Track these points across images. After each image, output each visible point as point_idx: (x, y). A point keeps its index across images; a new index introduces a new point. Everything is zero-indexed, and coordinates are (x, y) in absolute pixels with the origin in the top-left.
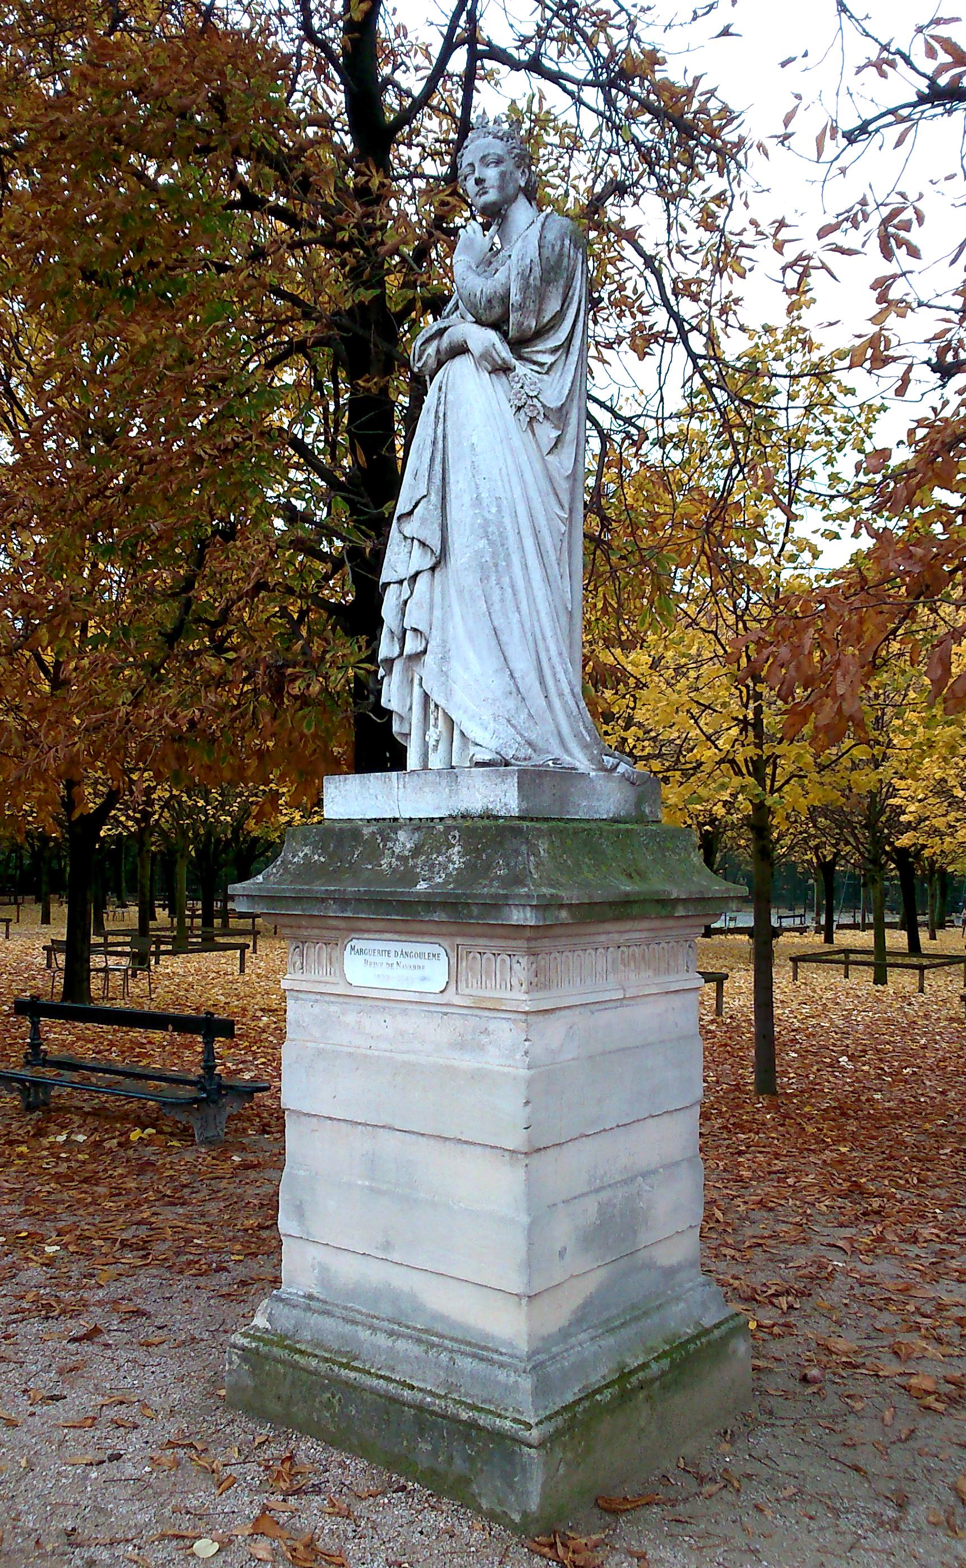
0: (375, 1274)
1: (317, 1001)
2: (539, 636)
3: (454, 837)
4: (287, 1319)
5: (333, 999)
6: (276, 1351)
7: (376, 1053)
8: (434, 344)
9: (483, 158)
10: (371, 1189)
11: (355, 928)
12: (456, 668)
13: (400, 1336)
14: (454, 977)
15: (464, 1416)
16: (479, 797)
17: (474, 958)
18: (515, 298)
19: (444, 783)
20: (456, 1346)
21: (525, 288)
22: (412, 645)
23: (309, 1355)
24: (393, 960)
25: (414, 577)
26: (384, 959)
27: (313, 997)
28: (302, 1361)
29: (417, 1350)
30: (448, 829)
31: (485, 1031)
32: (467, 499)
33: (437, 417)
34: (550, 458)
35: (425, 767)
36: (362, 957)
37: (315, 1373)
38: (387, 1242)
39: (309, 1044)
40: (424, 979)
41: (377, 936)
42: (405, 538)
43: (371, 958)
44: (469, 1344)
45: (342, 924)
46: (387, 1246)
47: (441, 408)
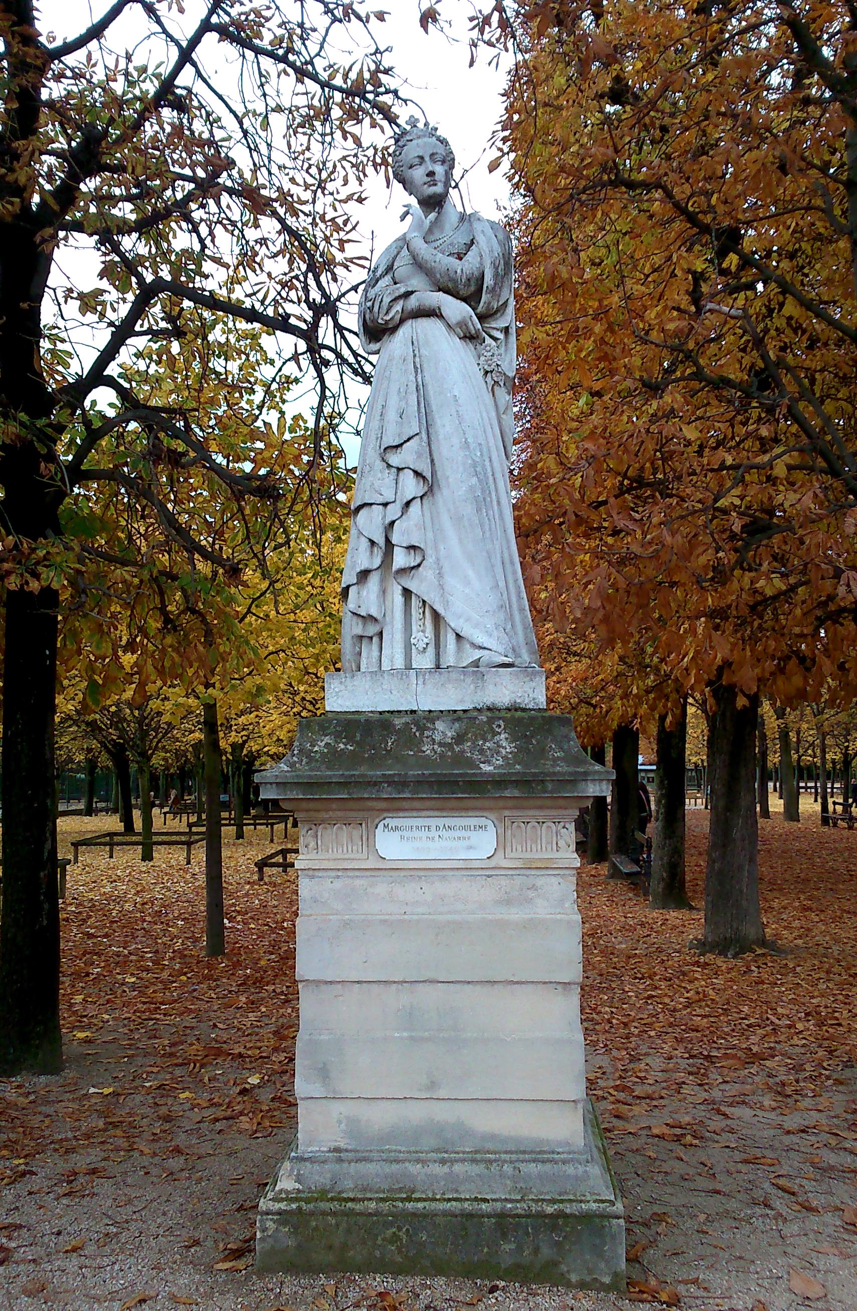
0: (416, 1114)
1: (338, 877)
2: (507, 561)
3: (499, 726)
5: (357, 873)
6: (324, 1206)
7: (415, 917)
8: (401, 302)
9: (432, 155)
10: (411, 1038)
11: (395, 807)
12: (451, 582)
13: (453, 1162)
14: (502, 844)
15: (550, 1209)
16: (507, 692)
17: (519, 827)
18: (488, 281)
20: (514, 1157)
21: (496, 275)
22: (400, 559)
23: (363, 1200)
24: (434, 833)
25: (408, 504)
26: (424, 834)
27: (333, 874)
28: (358, 1207)
29: (476, 1170)
30: (491, 721)
31: (534, 887)
32: (455, 441)
33: (415, 367)
34: (504, 416)
35: (409, 667)
36: (398, 834)
37: (377, 1213)
38: (432, 1082)
40: (470, 848)
41: (415, 814)
42: (389, 466)
43: (406, 834)
44: (524, 1152)
45: (383, 805)
46: (433, 1085)
47: (417, 359)
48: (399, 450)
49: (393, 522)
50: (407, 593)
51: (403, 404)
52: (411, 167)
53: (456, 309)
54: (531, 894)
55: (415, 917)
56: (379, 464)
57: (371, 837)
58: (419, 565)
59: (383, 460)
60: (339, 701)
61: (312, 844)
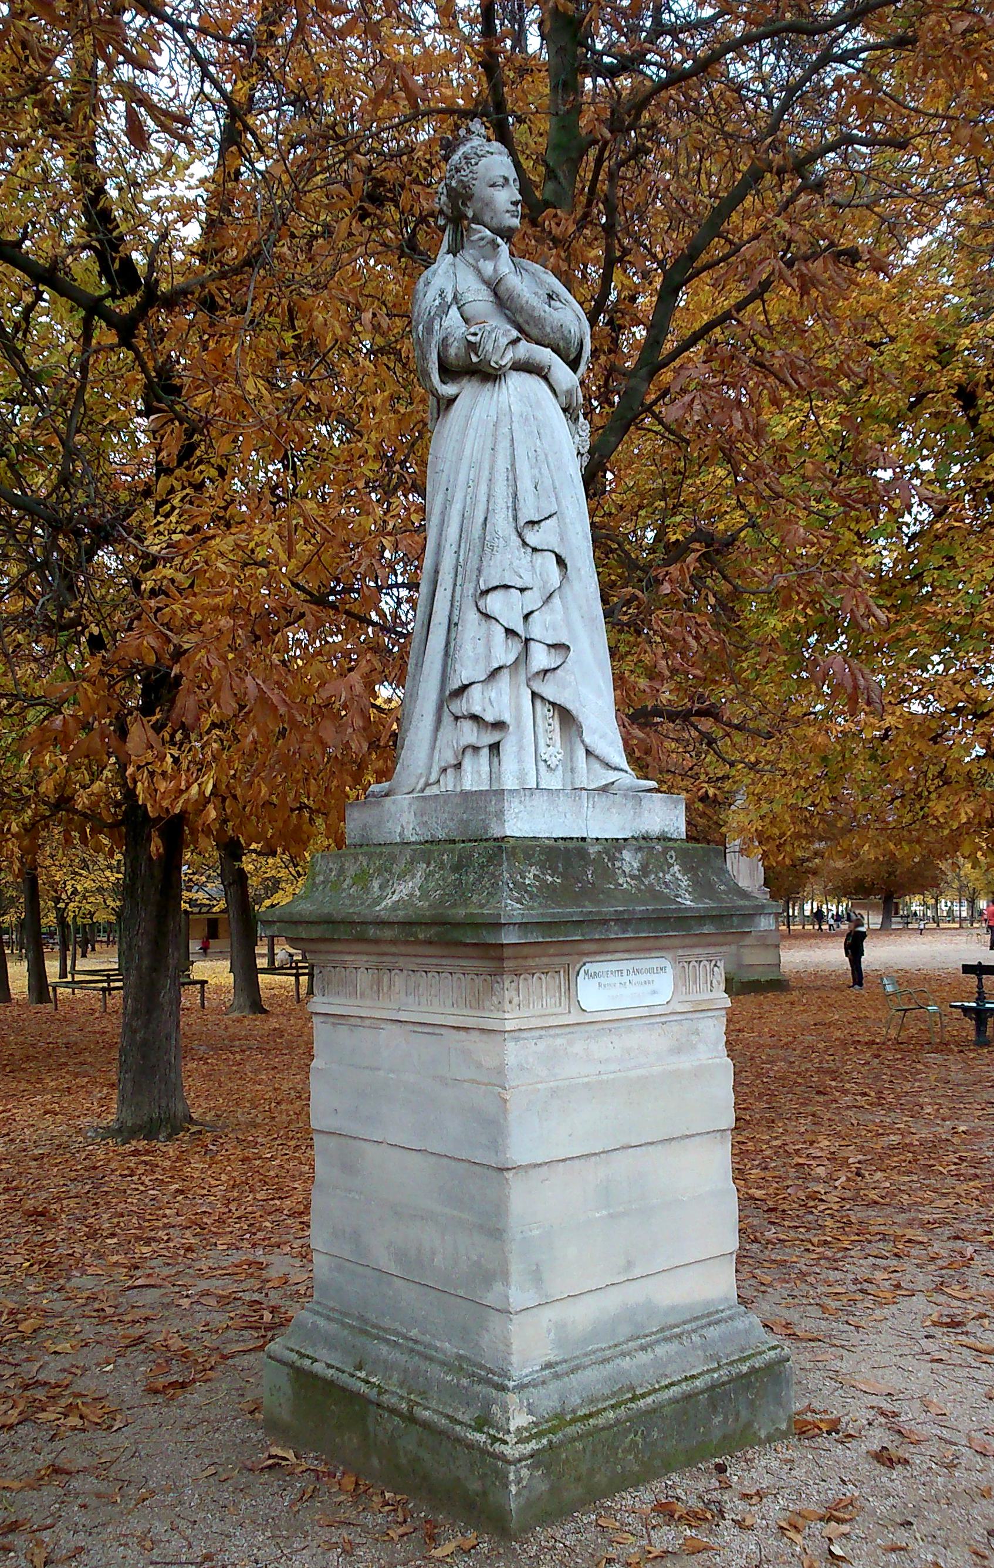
0: (612, 1302)
1: (541, 1037)
4: (547, 1400)
5: (558, 1031)
6: (570, 1430)
7: (612, 1076)
10: (611, 1216)
11: (604, 948)
13: (650, 1345)
15: (745, 1369)
19: (630, 805)
20: (694, 1325)
22: (541, 658)
23: (599, 1412)
24: (625, 979)
26: (616, 980)
27: (536, 1033)
28: (600, 1421)
29: (673, 1347)
30: (666, 850)
36: (597, 980)
37: (618, 1422)
38: (629, 1262)
39: (539, 1086)
40: (654, 992)
41: (609, 957)
42: (525, 544)
44: (697, 1318)
45: (593, 947)
46: (630, 1264)
48: (536, 527)
49: (532, 612)
50: (534, 695)
51: (536, 471)
52: (492, 186)
53: (564, 376)
54: (694, 1039)
55: (612, 1076)
56: (515, 541)
57: (572, 986)
58: (555, 669)
59: (520, 535)
60: (519, 825)
61: (515, 1001)
